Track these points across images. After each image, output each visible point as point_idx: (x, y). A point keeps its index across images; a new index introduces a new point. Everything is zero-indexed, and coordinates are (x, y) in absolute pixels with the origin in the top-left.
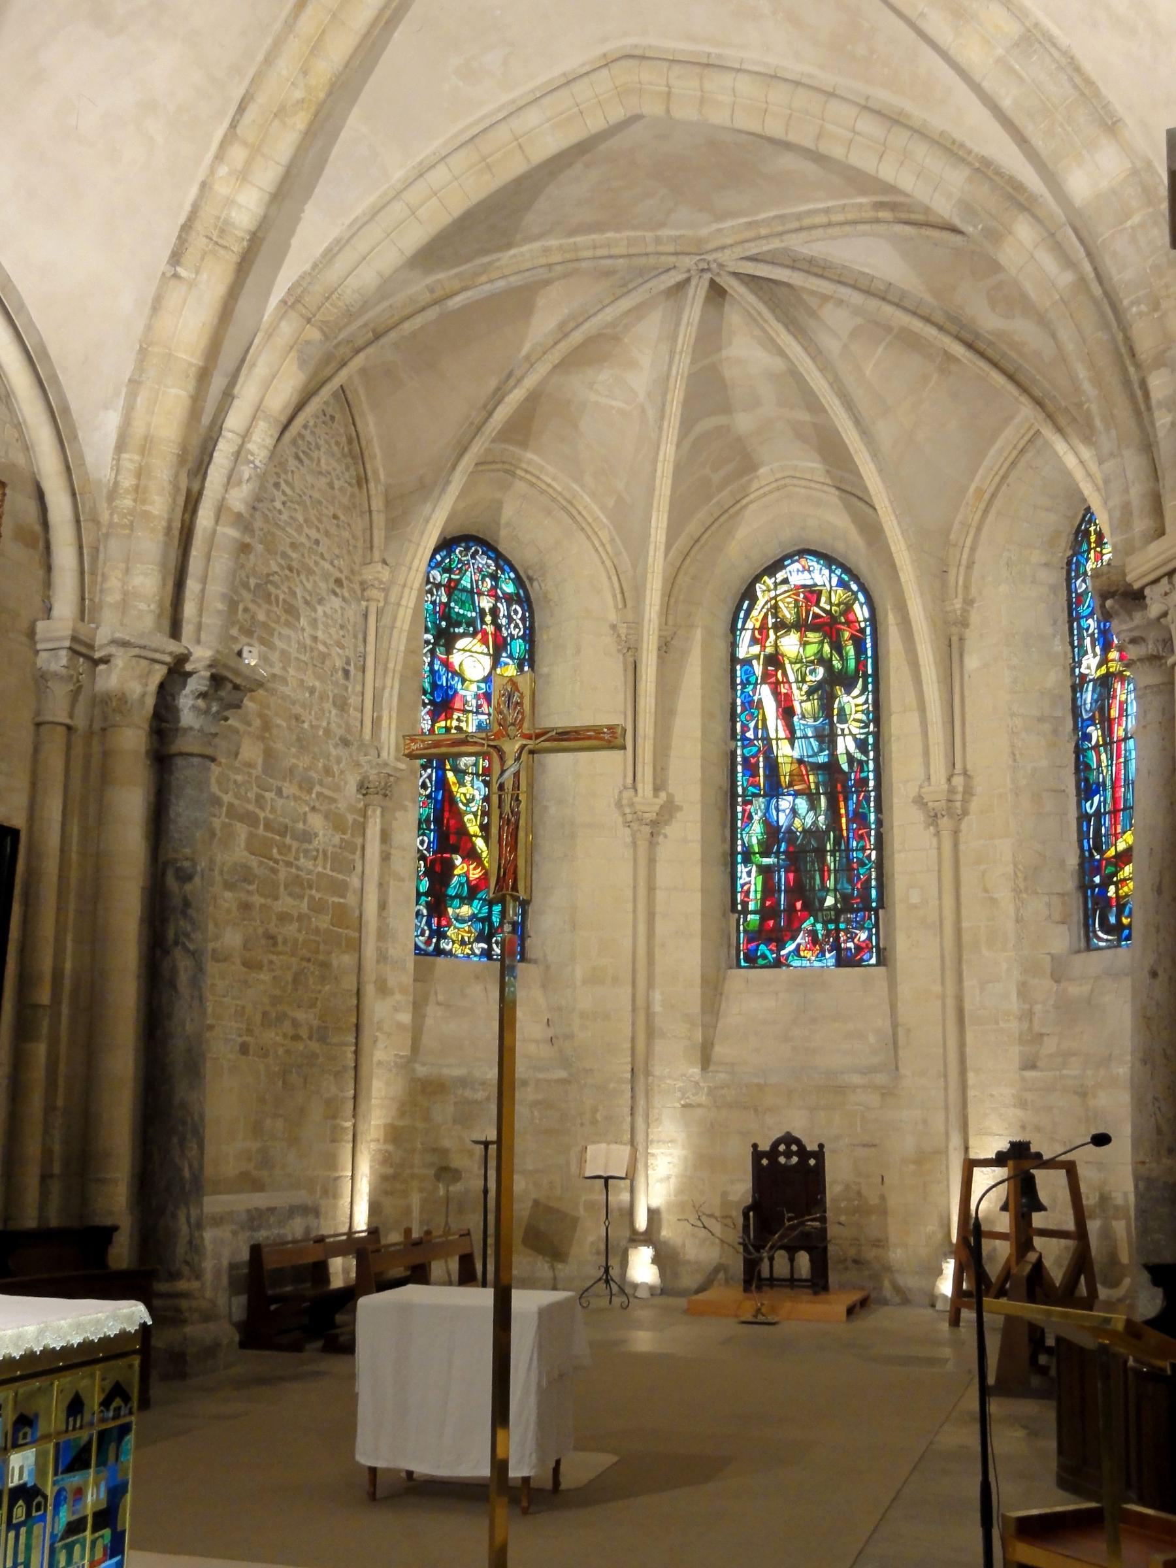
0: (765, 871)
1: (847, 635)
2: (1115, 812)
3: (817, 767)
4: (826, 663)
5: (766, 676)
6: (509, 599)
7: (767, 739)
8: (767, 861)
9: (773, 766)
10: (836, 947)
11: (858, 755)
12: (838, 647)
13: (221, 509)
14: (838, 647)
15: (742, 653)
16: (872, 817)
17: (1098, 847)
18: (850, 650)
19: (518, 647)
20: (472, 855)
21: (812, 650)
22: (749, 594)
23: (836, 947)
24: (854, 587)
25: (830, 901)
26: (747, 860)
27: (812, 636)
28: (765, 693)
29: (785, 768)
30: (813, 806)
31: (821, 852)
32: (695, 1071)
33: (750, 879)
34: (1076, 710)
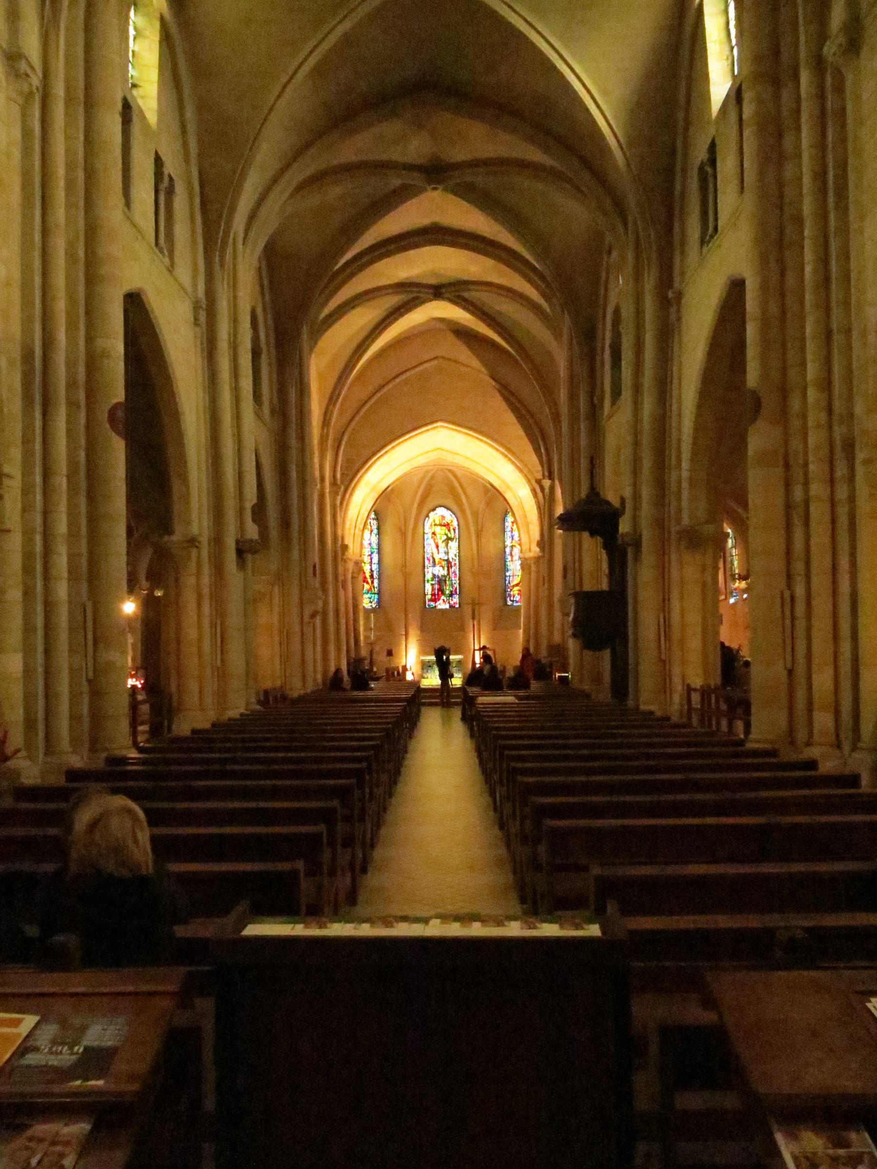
0: (432, 585)
1: (451, 528)
2: (513, 576)
3: (444, 560)
4: (446, 534)
5: (432, 537)
6: (373, 519)
7: (433, 553)
8: (433, 582)
9: (434, 559)
10: (449, 603)
11: (454, 558)
12: (449, 530)
13: (359, 529)
14: (449, 530)
15: (426, 531)
16: (457, 573)
17: (509, 583)
18: (452, 531)
19: (375, 531)
20: (367, 583)
21: (443, 532)
22: (427, 516)
23: (449, 603)
24: (453, 516)
25: (447, 592)
26: (428, 581)
27: (444, 528)
28: (431, 541)
29: (437, 561)
30: (444, 569)
31: (445, 581)
32: (419, 632)
33: (428, 588)
34: (505, 552)
